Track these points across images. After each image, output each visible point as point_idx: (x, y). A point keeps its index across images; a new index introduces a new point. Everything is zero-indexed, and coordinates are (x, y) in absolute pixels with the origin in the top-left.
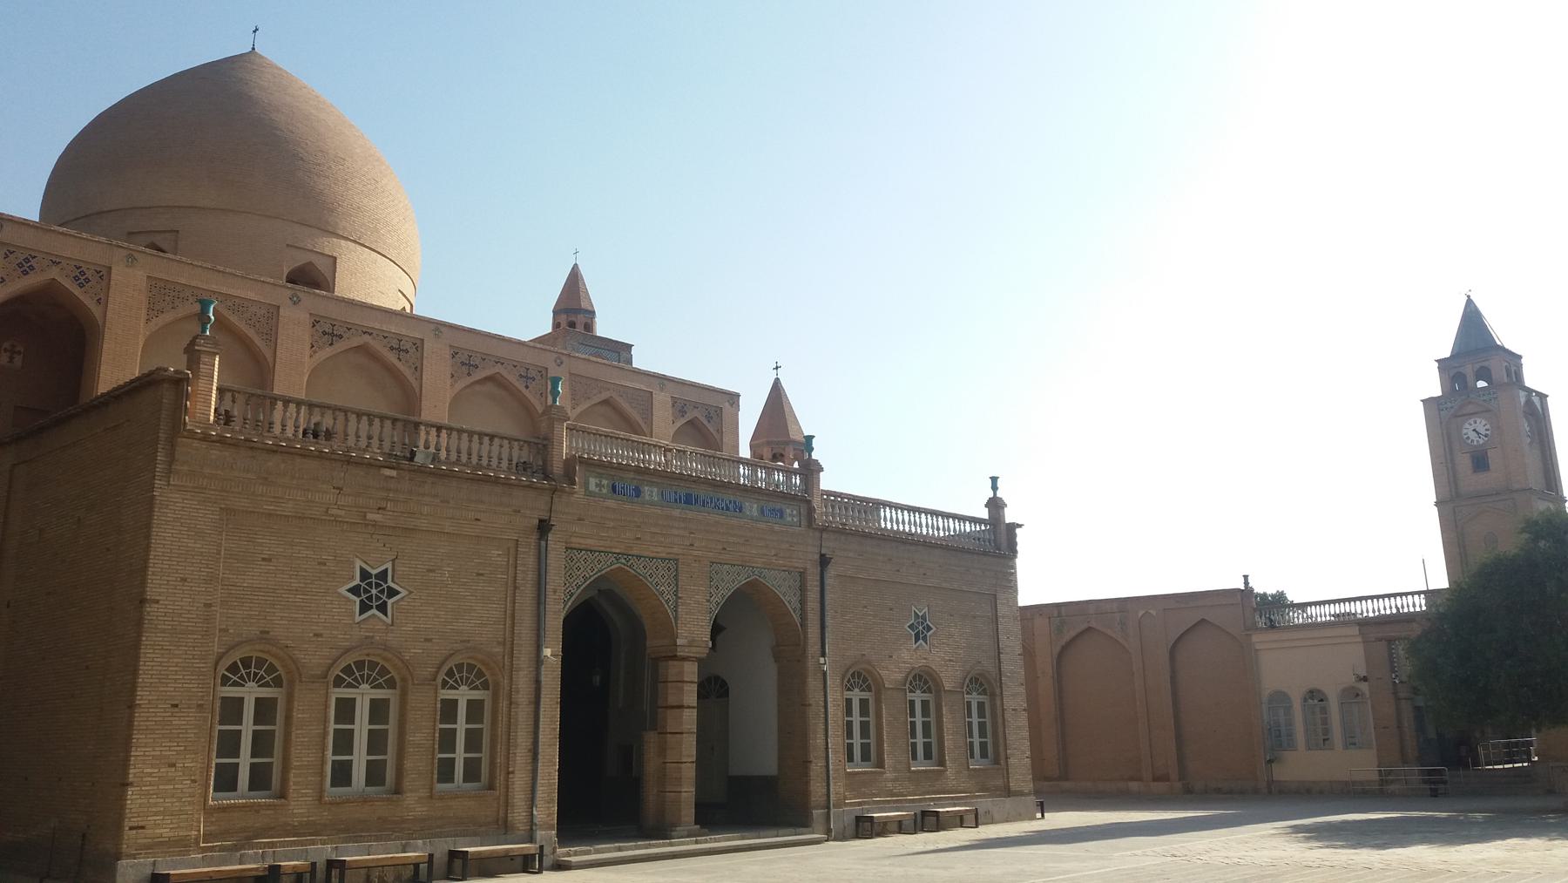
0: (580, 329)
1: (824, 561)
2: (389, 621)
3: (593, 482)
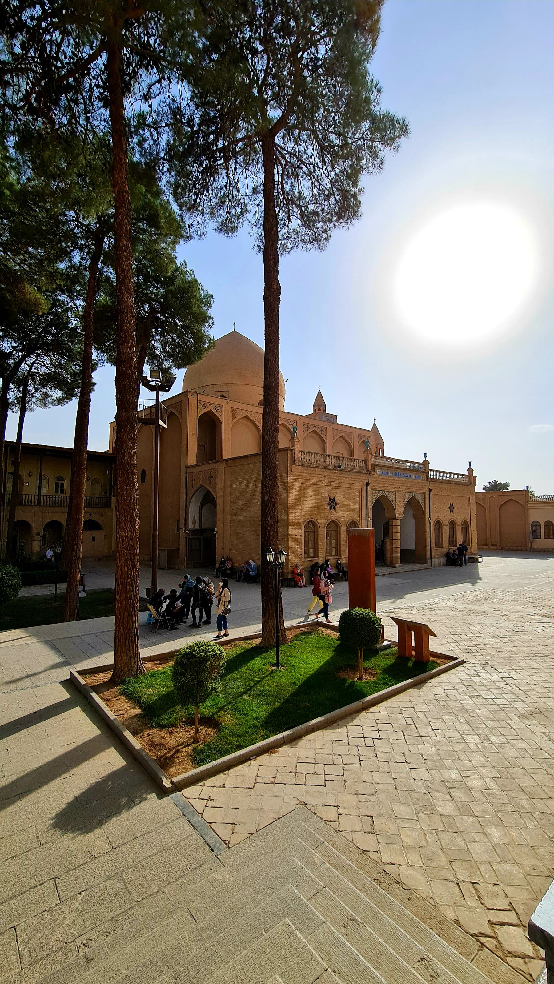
0: (322, 411)
1: (430, 490)
3: (377, 471)
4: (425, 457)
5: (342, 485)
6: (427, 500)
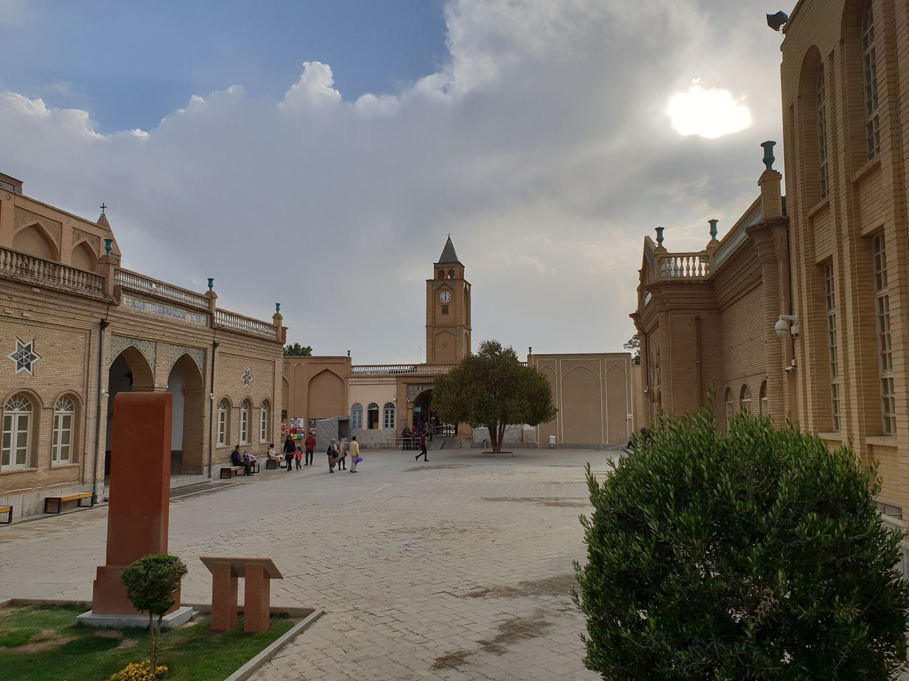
2: (31, 373)
4: (210, 286)
5: (49, 320)
6: (209, 362)
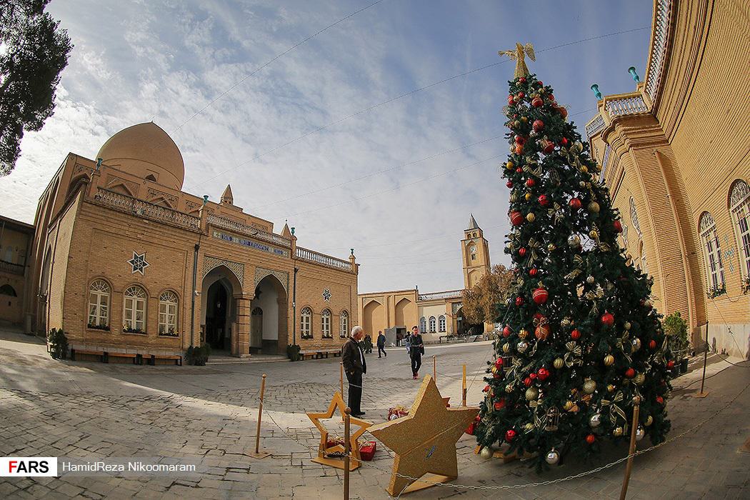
1: (296, 270)
6: (292, 281)
